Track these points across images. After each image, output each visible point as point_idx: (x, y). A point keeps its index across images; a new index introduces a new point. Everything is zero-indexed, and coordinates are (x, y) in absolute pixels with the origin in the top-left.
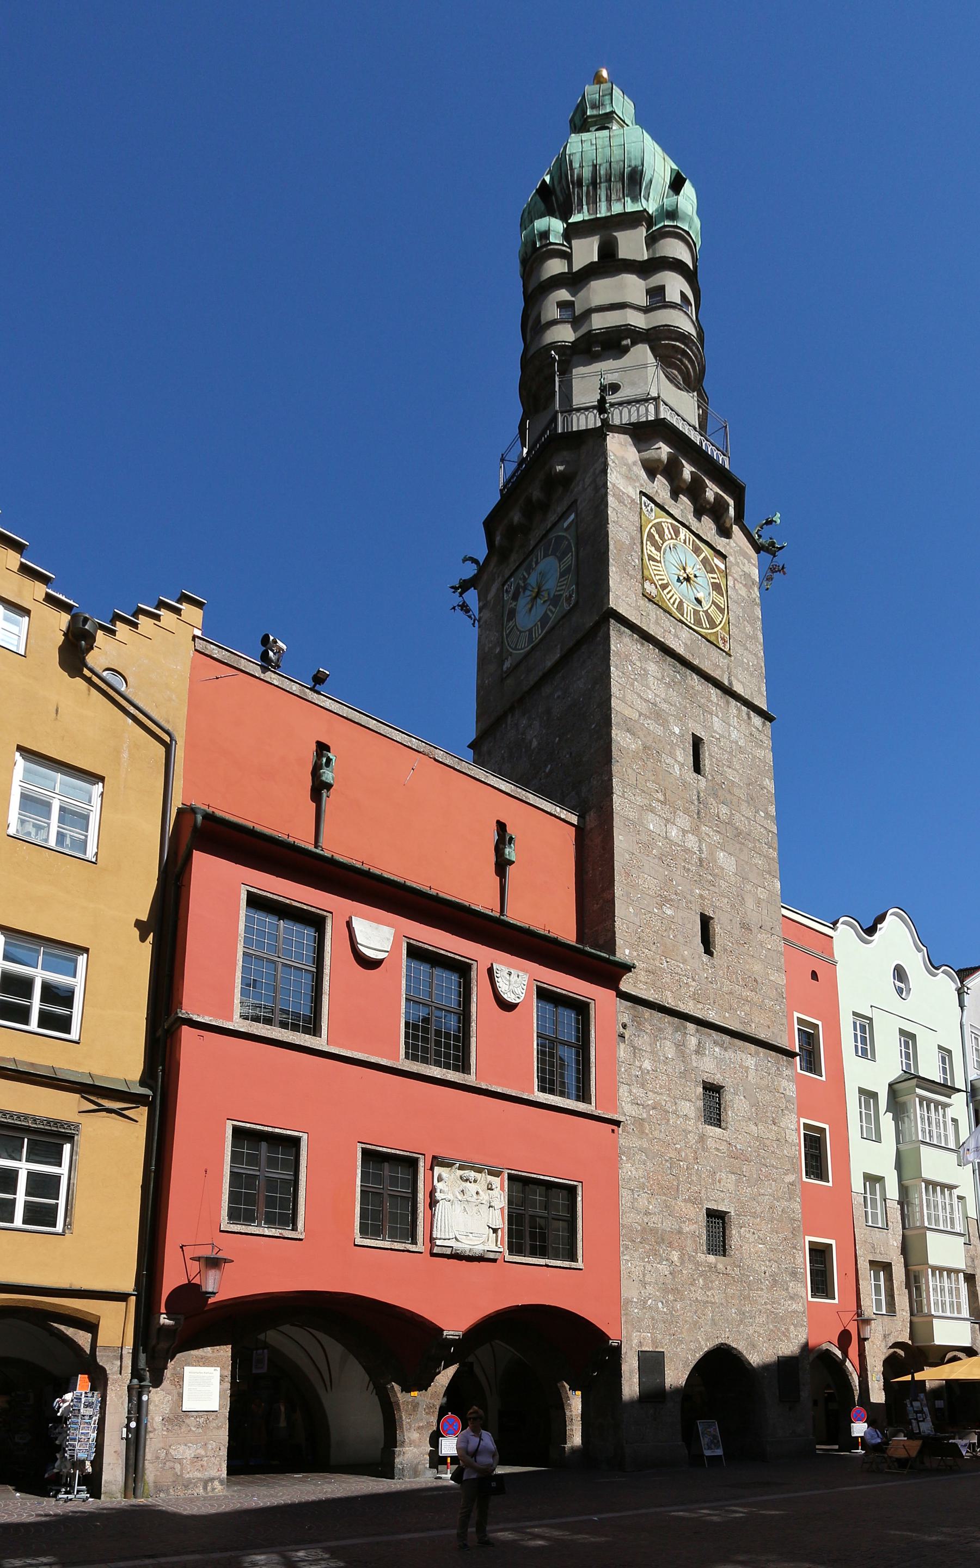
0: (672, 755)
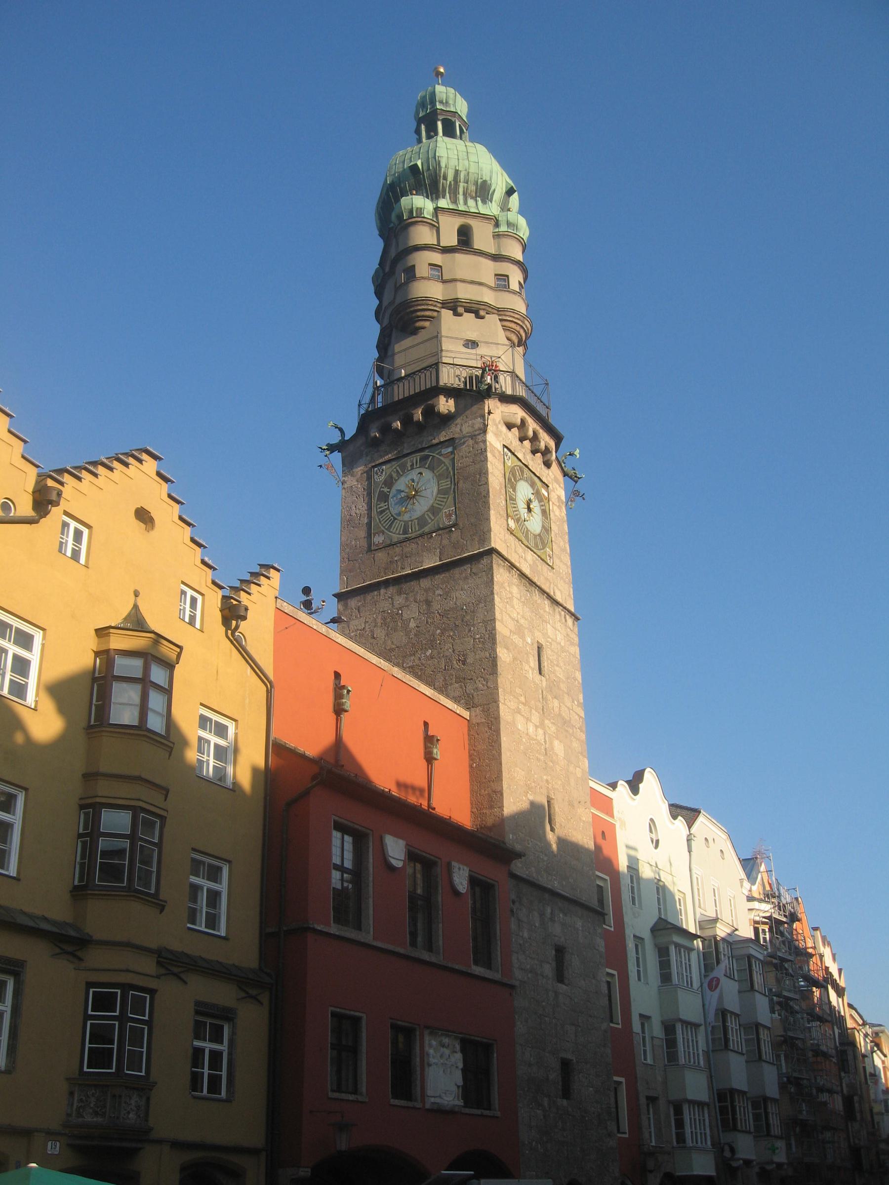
0: (528, 662)
